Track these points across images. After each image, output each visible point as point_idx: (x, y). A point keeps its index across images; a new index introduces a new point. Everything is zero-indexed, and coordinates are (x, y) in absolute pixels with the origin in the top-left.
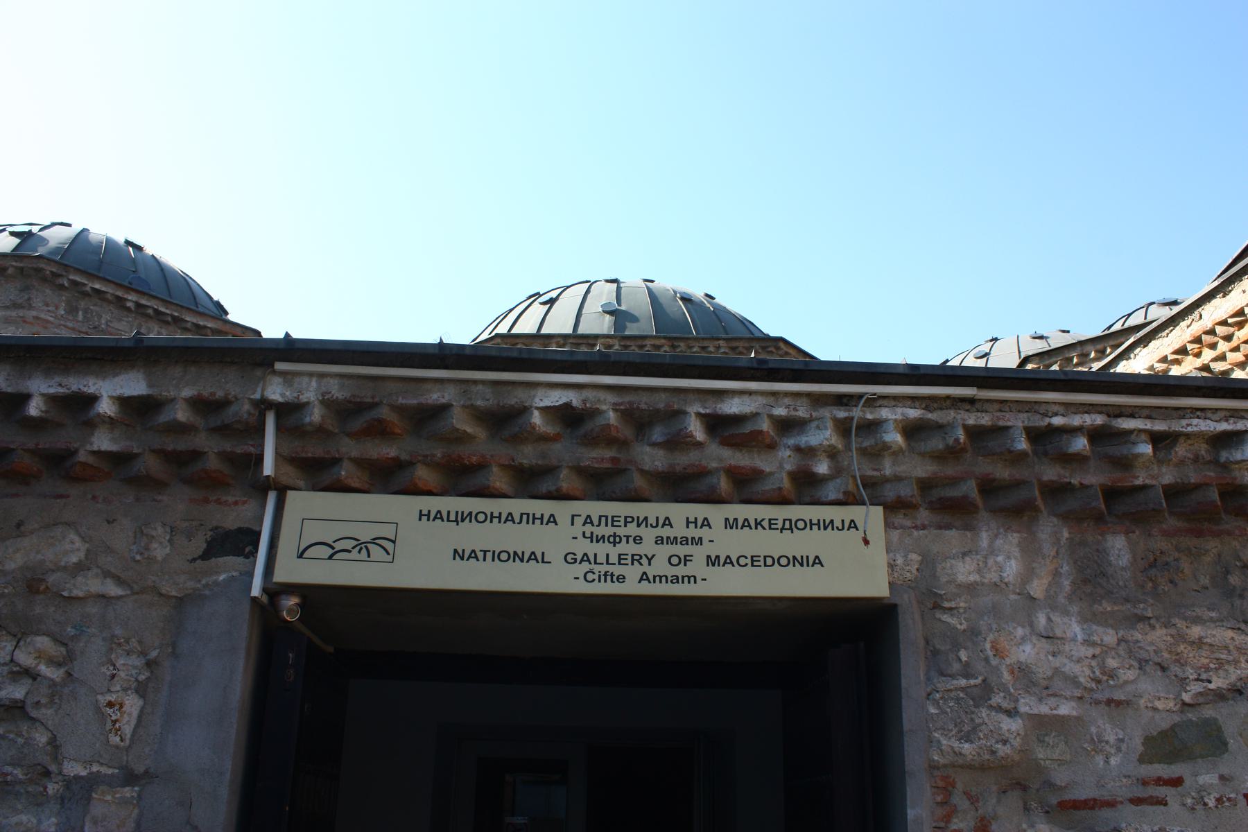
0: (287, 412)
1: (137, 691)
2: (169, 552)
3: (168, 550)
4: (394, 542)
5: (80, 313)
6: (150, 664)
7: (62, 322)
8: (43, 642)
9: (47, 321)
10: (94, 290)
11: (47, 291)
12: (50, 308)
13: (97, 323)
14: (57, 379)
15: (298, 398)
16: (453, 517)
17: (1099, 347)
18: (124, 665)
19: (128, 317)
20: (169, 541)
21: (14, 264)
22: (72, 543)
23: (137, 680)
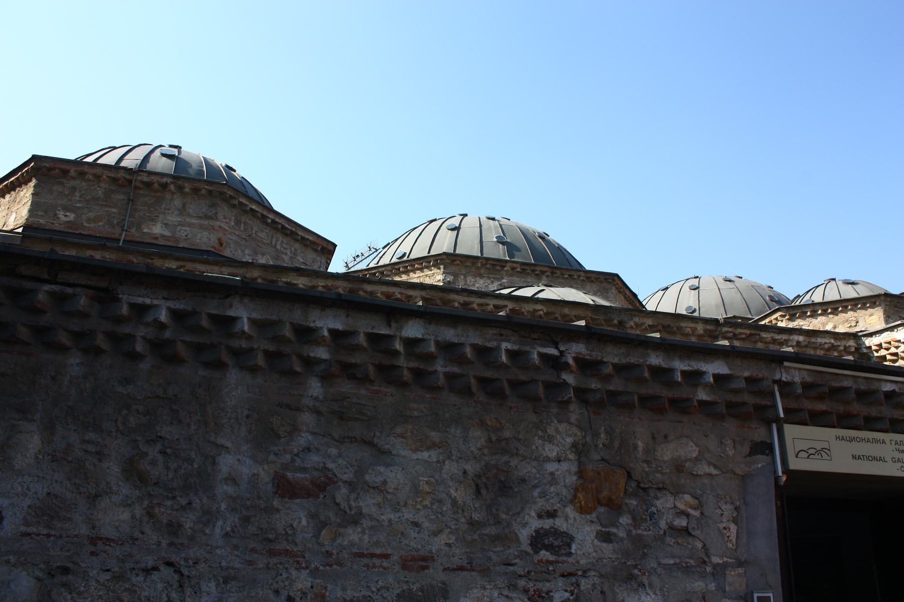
0: (785, 386)
1: (733, 521)
2: (734, 452)
3: (733, 451)
4: (829, 450)
5: (242, 224)
6: (737, 509)
7: (233, 231)
8: (687, 497)
9: (225, 230)
10: (251, 209)
11: (225, 208)
12: (227, 221)
13: (250, 233)
14: (687, 362)
15: (793, 380)
16: (848, 440)
17: (824, 308)
18: (725, 508)
19: (266, 229)
20: (733, 447)
21: (206, 187)
22: (691, 446)
23: (732, 517)
